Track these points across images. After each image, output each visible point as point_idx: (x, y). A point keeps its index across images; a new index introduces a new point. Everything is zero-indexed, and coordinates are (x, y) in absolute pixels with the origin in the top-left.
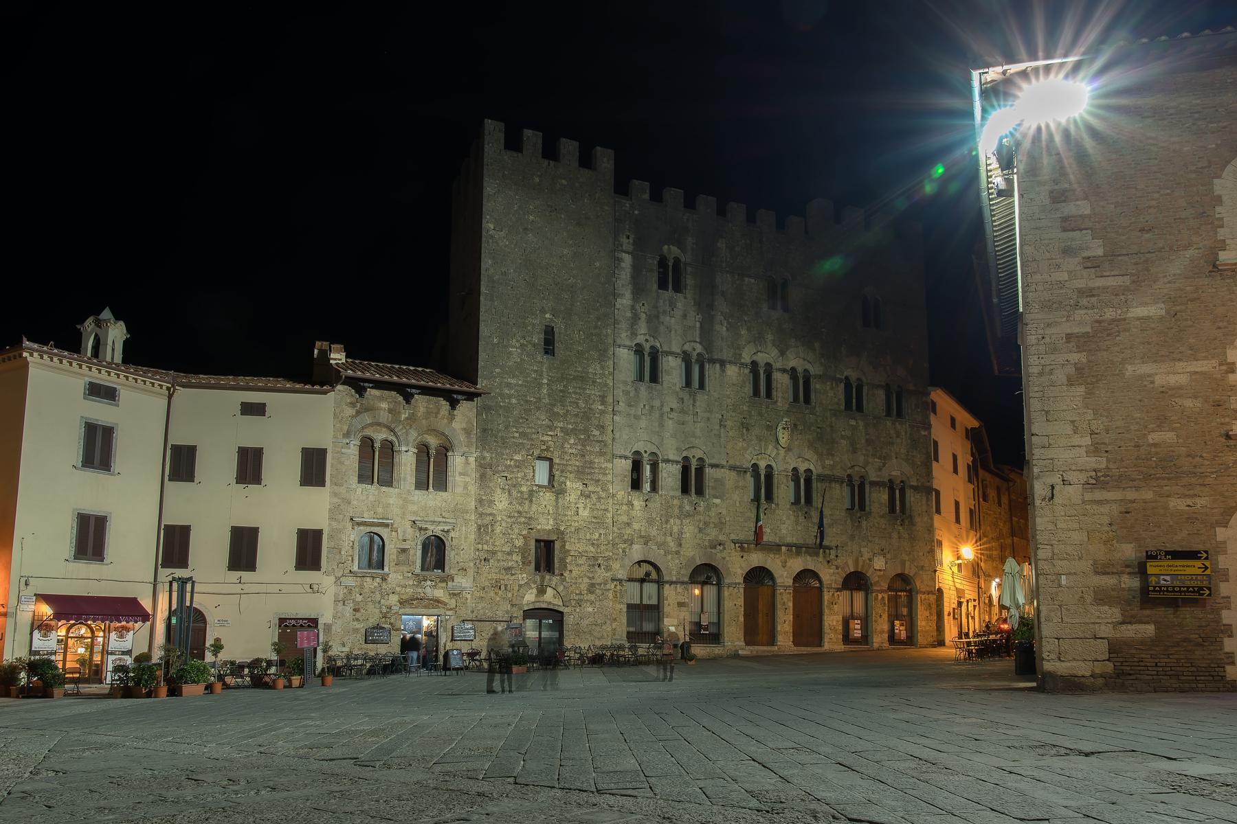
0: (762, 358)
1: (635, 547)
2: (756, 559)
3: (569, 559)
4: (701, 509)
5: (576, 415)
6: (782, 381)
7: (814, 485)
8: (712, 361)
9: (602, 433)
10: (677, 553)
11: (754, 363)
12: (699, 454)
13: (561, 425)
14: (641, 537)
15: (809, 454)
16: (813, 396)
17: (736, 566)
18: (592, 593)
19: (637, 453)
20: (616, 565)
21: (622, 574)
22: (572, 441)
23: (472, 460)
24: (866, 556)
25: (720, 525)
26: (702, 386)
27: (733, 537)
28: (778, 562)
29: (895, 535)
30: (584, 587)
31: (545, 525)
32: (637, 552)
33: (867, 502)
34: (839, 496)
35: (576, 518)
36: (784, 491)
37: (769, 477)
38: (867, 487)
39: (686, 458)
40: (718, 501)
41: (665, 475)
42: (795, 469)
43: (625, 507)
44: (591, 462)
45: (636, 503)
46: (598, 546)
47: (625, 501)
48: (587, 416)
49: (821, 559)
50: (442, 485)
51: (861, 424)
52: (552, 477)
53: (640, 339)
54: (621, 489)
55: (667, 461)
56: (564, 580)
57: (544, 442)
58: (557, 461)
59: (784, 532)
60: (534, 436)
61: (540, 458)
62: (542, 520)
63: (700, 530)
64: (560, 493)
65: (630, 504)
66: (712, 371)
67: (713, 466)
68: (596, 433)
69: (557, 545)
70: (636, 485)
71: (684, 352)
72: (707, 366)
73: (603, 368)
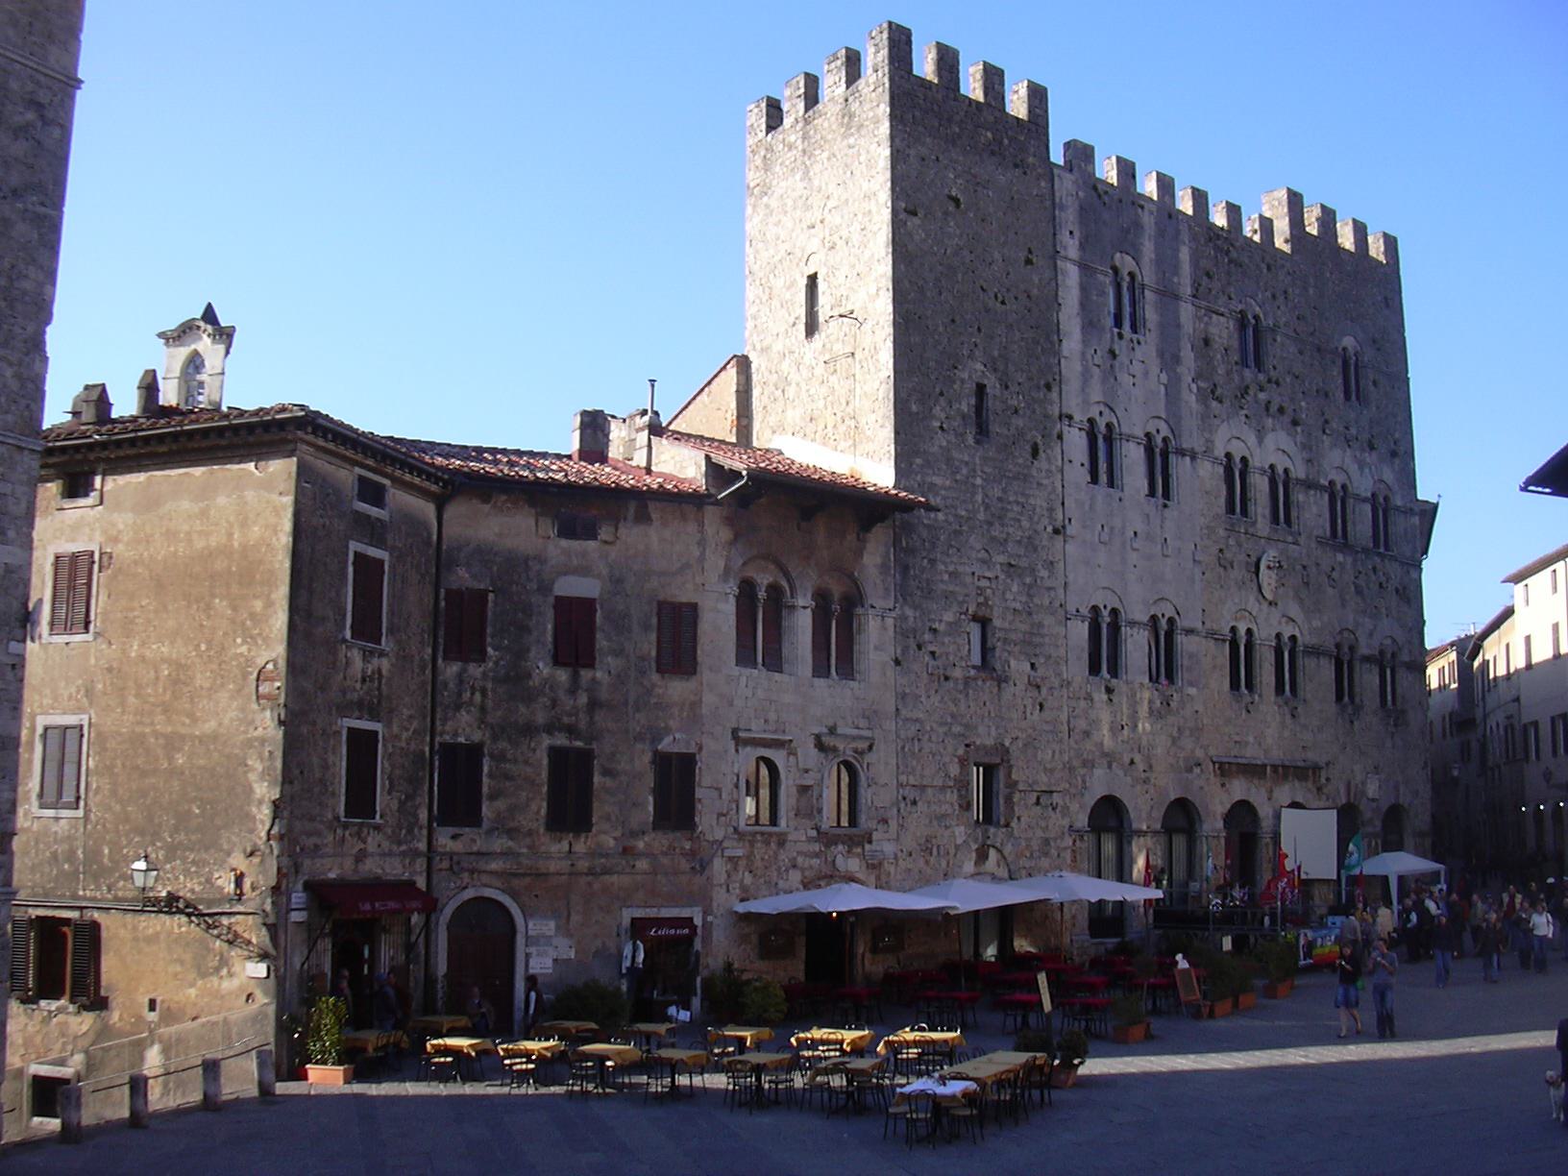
0: (1238, 450)
1: (1098, 772)
2: (1239, 789)
3: (1016, 797)
4: (1173, 705)
5: (1019, 542)
6: (1260, 484)
7: (1300, 662)
8: (1181, 452)
9: (1052, 574)
10: (1146, 781)
11: (1228, 455)
12: (1170, 612)
13: (1001, 559)
14: (1105, 755)
15: (1294, 610)
16: (1294, 514)
17: (1216, 802)
18: (1046, 854)
19: (1095, 609)
20: (1074, 807)
21: (1082, 821)
22: (1015, 588)
23: (890, 622)
24: (1359, 778)
25: (1197, 731)
26: (1166, 495)
27: (1212, 752)
28: (1263, 791)
29: (1389, 744)
30: (1035, 844)
31: (985, 736)
32: (1099, 784)
33: (1357, 690)
34: (1319, 676)
35: (1023, 725)
36: (1266, 675)
37: (1249, 646)
38: (1357, 665)
39: (1154, 618)
40: (1192, 691)
41: (1130, 647)
42: (1278, 636)
43: (1083, 704)
44: (1040, 625)
45: (1096, 696)
46: (1052, 771)
47: (1083, 694)
48: (1031, 544)
49: (1310, 784)
50: (847, 668)
51: (1349, 560)
52: (986, 651)
53: (1094, 412)
54: (1077, 668)
55: (1132, 624)
56: (1011, 835)
57: (981, 591)
58: (997, 623)
59: (1270, 741)
60: (969, 579)
61: (975, 618)
62: (981, 729)
63: (1174, 742)
64: (1001, 680)
65: (1089, 698)
66: (1180, 467)
67: (1189, 632)
68: (1044, 573)
69: (1001, 774)
70: (1094, 669)
71: (1148, 435)
72: (1172, 458)
73: (1049, 459)
